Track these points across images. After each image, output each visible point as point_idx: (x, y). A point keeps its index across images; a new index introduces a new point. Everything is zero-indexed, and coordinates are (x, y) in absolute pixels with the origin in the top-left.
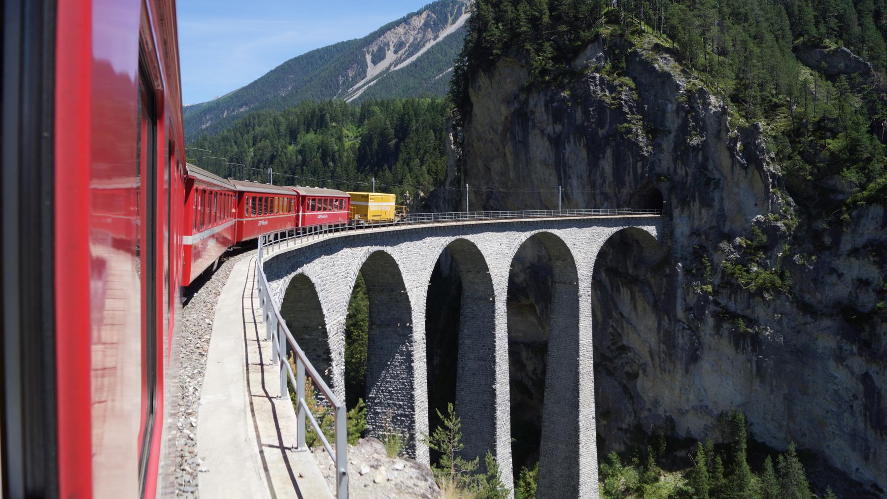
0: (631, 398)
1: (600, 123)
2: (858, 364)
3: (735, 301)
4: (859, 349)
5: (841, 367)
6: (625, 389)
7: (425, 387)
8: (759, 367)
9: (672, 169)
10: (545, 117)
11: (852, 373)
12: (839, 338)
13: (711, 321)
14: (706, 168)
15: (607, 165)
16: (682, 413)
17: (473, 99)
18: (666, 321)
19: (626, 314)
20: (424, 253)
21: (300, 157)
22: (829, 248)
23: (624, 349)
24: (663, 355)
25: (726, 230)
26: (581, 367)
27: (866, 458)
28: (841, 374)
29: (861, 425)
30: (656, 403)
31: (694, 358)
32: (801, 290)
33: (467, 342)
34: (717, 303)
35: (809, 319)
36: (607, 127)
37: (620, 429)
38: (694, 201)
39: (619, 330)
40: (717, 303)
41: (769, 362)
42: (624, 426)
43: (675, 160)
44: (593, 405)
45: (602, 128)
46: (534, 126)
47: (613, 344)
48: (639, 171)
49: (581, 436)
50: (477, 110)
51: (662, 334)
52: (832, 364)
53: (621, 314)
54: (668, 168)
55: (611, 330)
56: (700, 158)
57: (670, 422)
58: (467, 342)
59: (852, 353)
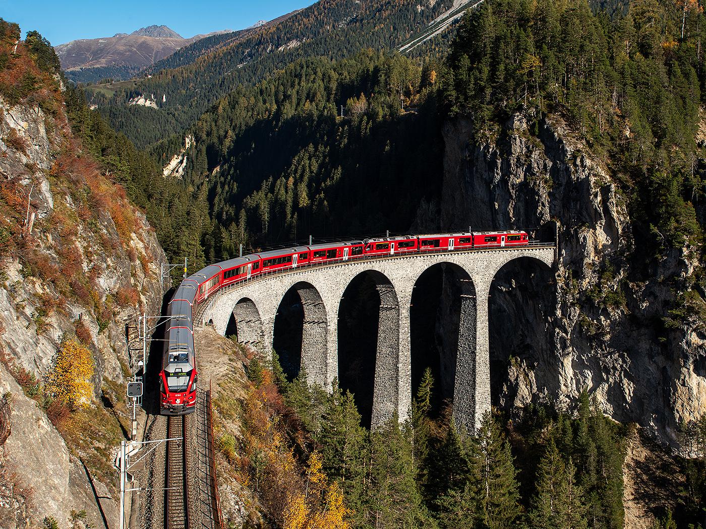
2: (660, 359)
3: (593, 313)
4: (661, 349)
5: (651, 363)
7: (336, 358)
9: (562, 212)
10: (484, 164)
11: (658, 366)
12: (650, 341)
14: (582, 215)
17: (445, 139)
20: (338, 280)
24: (549, 352)
26: (477, 357)
28: (652, 368)
32: (633, 306)
33: (382, 335)
38: (573, 238)
39: (526, 332)
43: (563, 207)
44: (489, 386)
46: (477, 171)
47: (521, 343)
49: (477, 407)
50: (447, 149)
51: (548, 336)
52: (646, 359)
53: (527, 321)
54: (560, 212)
55: (520, 332)
59: (659, 354)
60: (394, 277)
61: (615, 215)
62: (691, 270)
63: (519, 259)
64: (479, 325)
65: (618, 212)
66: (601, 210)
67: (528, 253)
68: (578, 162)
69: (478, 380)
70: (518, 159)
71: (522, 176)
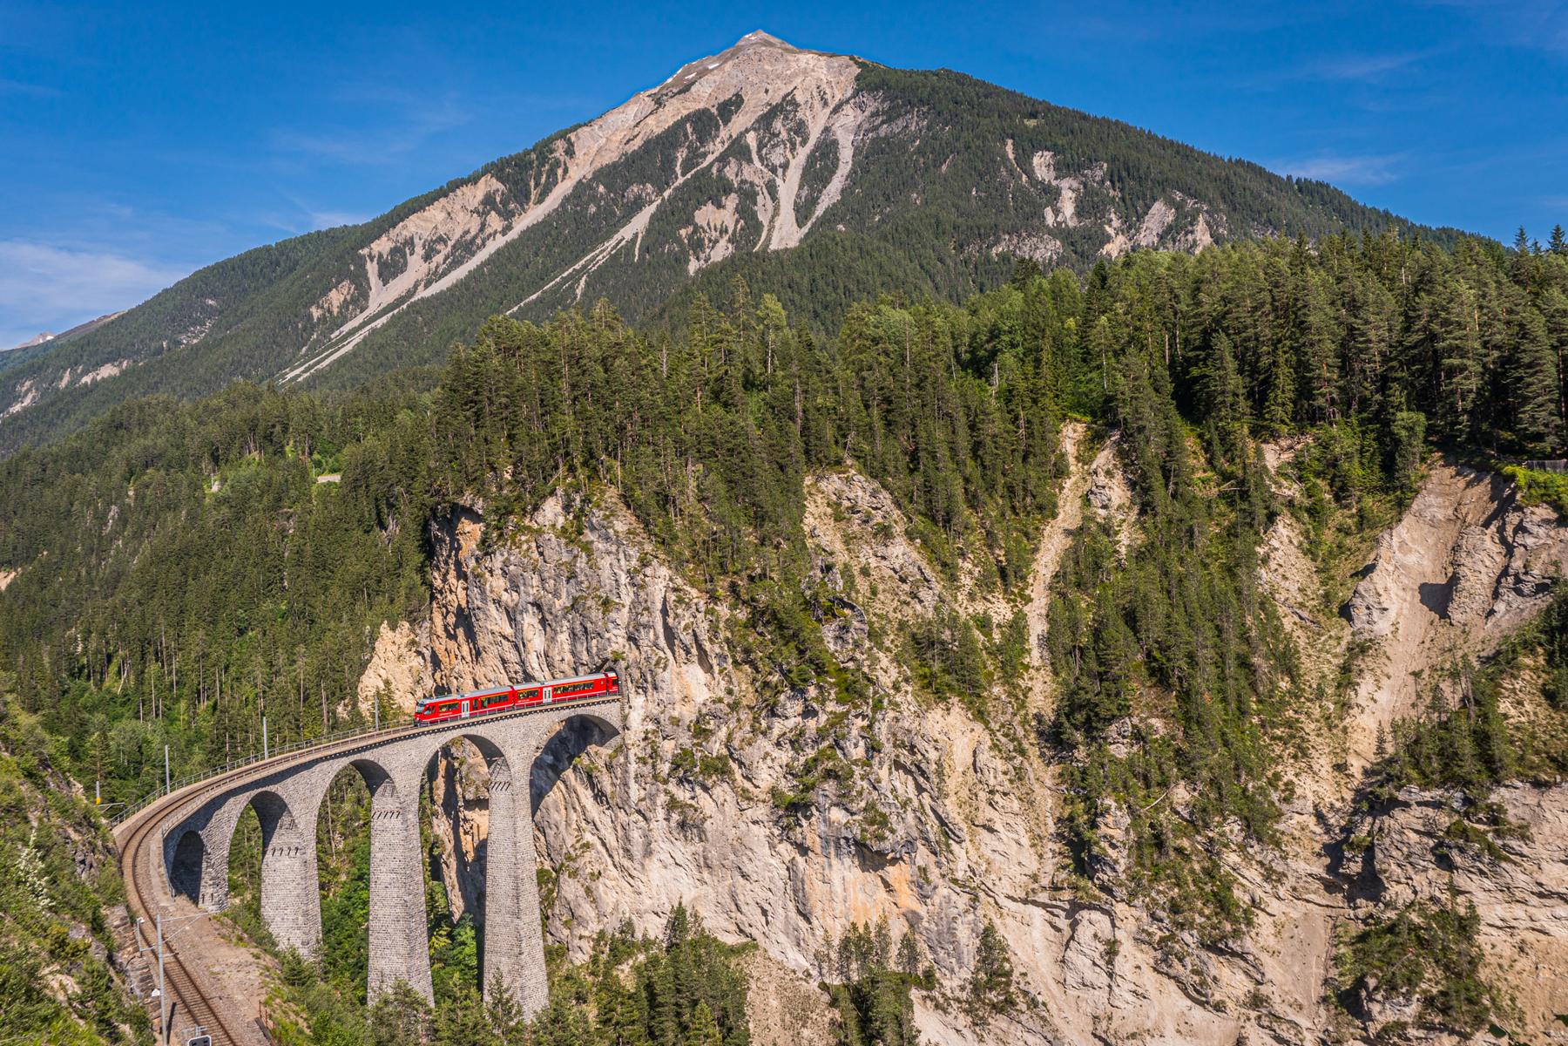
0: (594, 901)
1: (556, 594)
2: (785, 849)
6: (588, 891)
8: (705, 858)
13: (661, 813)
15: (564, 637)
16: (640, 914)
18: (621, 814)
19: (589, 807)
21: (225, 510)
22: (764, 733)
23: (587, 846)
25: (676, 714)
27: (798, 945)
29: (793, 914)
30: (617, 905)
31: (648, 853)
33: (379, 855)
34: (667, 792)
35: (744, 805)
36: (564, 595)
37: (581, 938)
40: (667, 792)
41: (713, 855)
42: (587, 933)
45: (559, 598)
48: (594, 650)
56: (652, 636)
57: (628, 927)
58: (379, 855)
60: (394, 765)
61: (707, 646)
62: (823, 718)
63: (569, 721)
64: (520, 824)
66: (688, 639)
67: (580, 711)
68: (648, 571)
69: (523, 905)
70: (558, 566)
71: (564, 595)
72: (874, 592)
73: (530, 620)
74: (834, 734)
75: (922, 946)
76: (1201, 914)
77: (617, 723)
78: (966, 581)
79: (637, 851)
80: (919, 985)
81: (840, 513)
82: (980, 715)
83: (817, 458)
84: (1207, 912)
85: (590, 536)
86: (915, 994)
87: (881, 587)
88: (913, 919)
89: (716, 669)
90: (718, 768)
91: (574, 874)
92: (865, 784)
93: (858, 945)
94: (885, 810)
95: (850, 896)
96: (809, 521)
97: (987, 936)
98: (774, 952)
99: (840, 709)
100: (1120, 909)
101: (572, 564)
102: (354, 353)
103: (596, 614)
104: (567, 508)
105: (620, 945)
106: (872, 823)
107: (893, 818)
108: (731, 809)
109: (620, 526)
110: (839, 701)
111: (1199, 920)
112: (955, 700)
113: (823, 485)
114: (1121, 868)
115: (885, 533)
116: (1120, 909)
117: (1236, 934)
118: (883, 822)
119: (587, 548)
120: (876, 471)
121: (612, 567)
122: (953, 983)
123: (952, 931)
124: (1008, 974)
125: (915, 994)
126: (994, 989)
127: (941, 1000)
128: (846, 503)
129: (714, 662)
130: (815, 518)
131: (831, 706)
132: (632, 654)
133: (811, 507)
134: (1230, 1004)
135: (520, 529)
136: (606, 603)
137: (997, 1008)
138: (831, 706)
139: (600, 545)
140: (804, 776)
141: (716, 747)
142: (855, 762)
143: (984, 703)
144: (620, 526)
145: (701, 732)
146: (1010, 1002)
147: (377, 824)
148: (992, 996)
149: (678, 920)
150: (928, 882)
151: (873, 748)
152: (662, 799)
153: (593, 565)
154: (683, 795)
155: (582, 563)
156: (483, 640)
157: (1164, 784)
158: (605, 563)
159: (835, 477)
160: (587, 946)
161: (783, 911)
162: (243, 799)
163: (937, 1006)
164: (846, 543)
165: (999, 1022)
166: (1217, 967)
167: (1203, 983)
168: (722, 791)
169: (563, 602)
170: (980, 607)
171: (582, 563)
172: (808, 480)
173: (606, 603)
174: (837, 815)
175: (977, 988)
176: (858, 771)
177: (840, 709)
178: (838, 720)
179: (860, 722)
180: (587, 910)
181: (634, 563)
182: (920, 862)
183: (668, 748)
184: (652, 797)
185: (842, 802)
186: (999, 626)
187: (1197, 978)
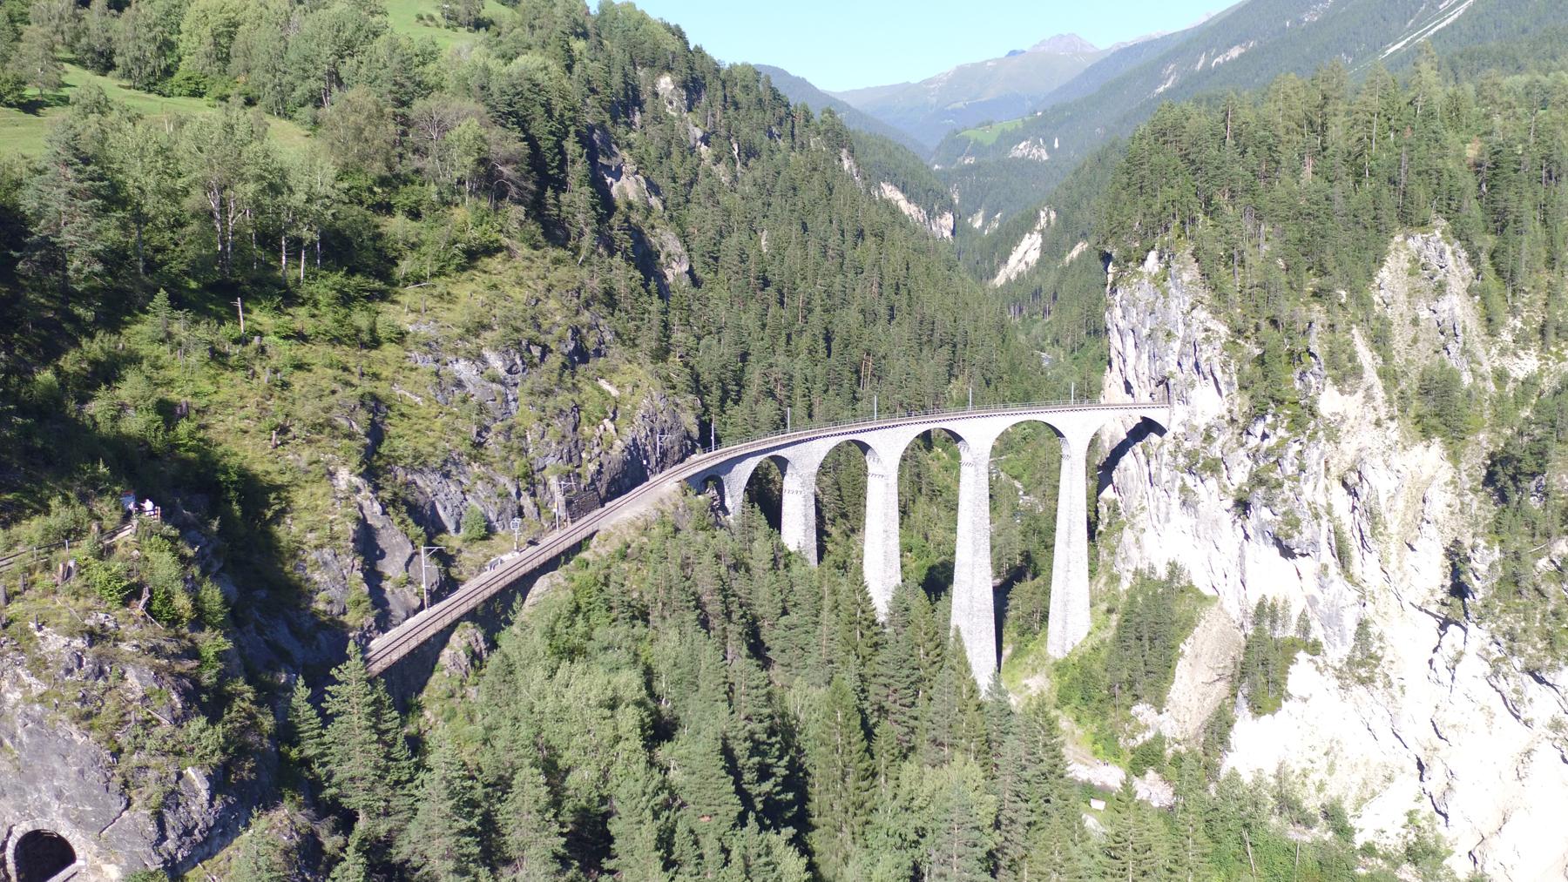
1: (1144, 326)
15: (1145, 357)
23: (1143, 509)
25: (1195, 423)
31: (1168, 520)
41: (1201, 528)
57: (1152, 569)
61: (1218, 374)
65: (1224, 372)
72: (1415, 341)
73: (1130, 341)
74: (1276, 456)
75: (1315, 624)
76: (1534, 647)
77: (1164, 424)
78: (1506, 337)
79: (1162, 516)
80: (1306, 648)
81: (1418, 266)
82: (1454, 457)
83: (1410, 219)
84: (1539, 646)
85: (1169, 283)
86: (1302, 656)
87: (1422, 336)
88: (1312, 601)
89: (1225, 393)
90: (1214, 467)
91: (1132, 527)
92: (1292, 495)
93: (1265, 613)
94: (1300, 516)
95: (1272, 577)
96: (1384, 274)
97: (1363, 625)
98: (1225, 606)
99: (1287, 435)
100: (1472, 627)
101: (1154, 303)
102: (1452, 26)
103: (1161, 343)
104: (1160, 258)
105: (1144, 579)
106: (1286, 524)
107: (1304, 523)
108: (1215, 498)
109: (1186, 277)
110: (1288, 429)
111: (1530, 650)
112: (1438, 440)
113: (1410, 241)
114: (1479, 596)
115: (1441, 289)
116: (1472, 627)
117: (1551, 667)
118: (1295, 524)
119: (1165, 294)
120: (1460, 235)
121: (1178, 304)
122: (1338, 651)
123: (1339, 616)
124: (1379, 659)
125: (1302, 656)
126: (1364, 665)
127: (1321, 665)
128: (1423, 260)
129: (1222, 386)
130: (1390, 276)
131: (1281, 432)
132: (1180, 376)
133: (1390, 261)
134: (1537, 724)
135: (1136, 273)
136: (1169, 334)
137: (1362, 681)
138: (1281, 432)
139: (1173, 290)
140: (1258, 480)
141: (1215, 451)
142: (1288, 478)
143: (1464, 447)
144: (1186, 277)
145: (1208, 438)
146: (1371, 680)
147: (963, 468)
148: (1363, 672)
149: (1174, 570)
150: (1326, 575)
151: (1302, 469)
152: (1178, 483)
153: (1166, 306)
154: (1190, 481)
155: (1159, 304)
156: (1113, 354)
157: (1548, 535)
158: (1173, 305)
159: (1419, 236)
160: (1130, 576)
161: (1235, 577)
162: (832, 442)
163: (1317, 668)
164: (1410, 296)
165: (1359, 691)
166: (1532, 687)
167: (1520, 701)
168: (1212, 483)
169: (1145, 332)
170: (1508, 362)
171: (1159, 304)
172: (1399, 238)
173: (1169, 334)
174: (1266, 514)
175: (1350, 661)
176: (1287, 485)
177: (1287, 435)
178: (1283, 443)
179: (1297, 447)
180: (1134, 553)
181: (1187, 307)
182: (1323, 561)
183: (1188, 445)
184: (1173, 481)
185: (1269, 503)
186: (1515, 380)
187: (1515, 696)
